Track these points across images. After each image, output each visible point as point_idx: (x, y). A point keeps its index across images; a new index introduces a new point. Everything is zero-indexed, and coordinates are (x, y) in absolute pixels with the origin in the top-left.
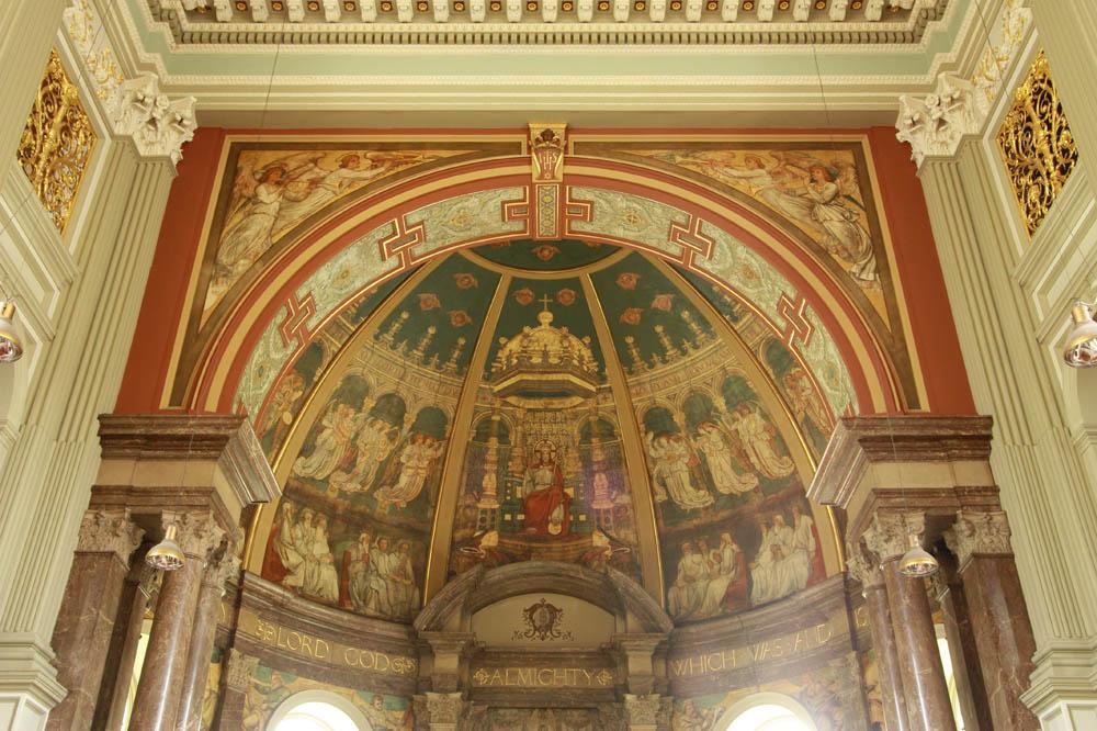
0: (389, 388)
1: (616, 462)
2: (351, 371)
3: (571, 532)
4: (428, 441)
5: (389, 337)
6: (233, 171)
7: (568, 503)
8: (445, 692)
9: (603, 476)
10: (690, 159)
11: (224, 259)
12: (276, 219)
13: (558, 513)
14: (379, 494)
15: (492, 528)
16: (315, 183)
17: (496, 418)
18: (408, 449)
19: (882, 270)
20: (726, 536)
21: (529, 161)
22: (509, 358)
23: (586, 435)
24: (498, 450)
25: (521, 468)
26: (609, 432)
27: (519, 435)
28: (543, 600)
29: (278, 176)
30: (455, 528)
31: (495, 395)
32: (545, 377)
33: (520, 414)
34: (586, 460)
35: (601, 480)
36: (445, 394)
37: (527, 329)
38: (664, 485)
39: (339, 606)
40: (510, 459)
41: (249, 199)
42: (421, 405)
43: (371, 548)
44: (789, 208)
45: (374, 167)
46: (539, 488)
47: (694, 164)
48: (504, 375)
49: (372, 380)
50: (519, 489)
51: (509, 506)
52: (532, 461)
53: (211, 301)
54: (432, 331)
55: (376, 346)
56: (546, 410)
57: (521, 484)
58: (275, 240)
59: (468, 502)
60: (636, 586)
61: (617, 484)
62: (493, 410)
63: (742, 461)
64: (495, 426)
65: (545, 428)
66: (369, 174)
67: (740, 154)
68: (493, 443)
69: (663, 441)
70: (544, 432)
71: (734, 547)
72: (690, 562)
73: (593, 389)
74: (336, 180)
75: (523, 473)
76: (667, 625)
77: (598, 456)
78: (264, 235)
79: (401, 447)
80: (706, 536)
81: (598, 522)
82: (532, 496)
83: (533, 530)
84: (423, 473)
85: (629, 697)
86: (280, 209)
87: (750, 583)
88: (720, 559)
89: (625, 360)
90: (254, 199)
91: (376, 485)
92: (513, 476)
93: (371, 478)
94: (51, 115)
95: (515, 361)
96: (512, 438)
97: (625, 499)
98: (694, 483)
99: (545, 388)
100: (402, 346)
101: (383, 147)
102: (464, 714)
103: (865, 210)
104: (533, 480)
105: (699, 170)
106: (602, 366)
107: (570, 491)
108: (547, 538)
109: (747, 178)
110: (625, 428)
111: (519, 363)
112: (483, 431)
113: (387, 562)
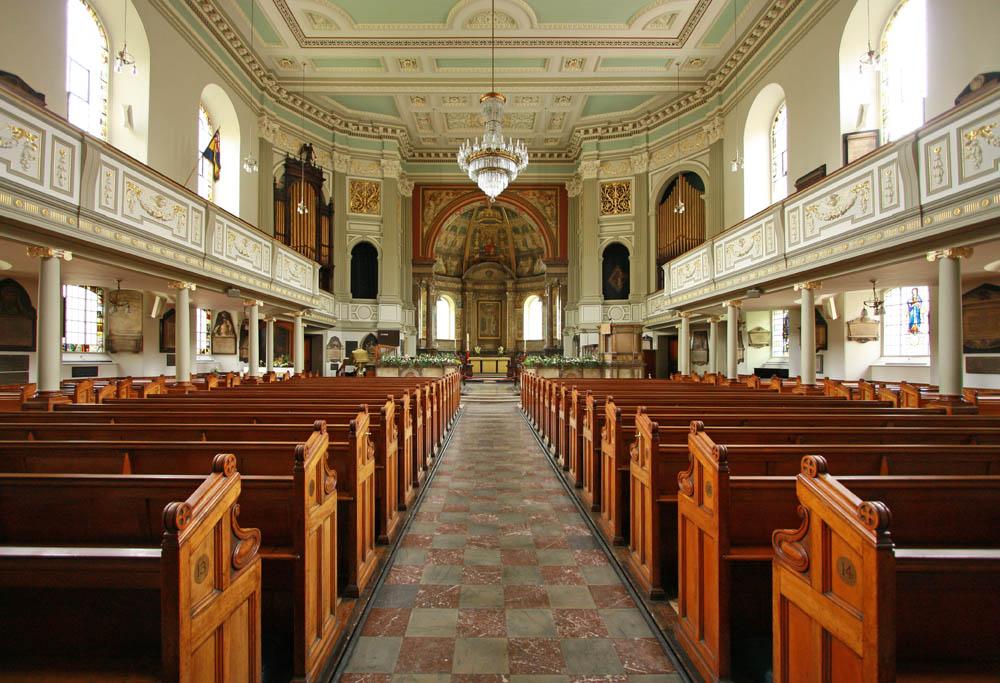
1: (505, 239)
6: (423, 197)
11: (426, 220)
13: (492, 250)
16: (441, 200)
19: (557, 224)
23: (499, 232)
26: (505, 232)
29: (433, 198)
34: (499, 238)
35: (502, 243)
39: (446, 275)
44: (539, 207)
51: (481, 248)
52: (486, 238)
53: (425, 231)
63: (534, 242)
67: (531, 192)
74: (446, 198)
77: (502, 237)
80: (525, 257)
81: (502, 252)
90: (429, 204)
101: (455, 190)
108: (489, 255)
110: (509, 231)
113: (455, 263)
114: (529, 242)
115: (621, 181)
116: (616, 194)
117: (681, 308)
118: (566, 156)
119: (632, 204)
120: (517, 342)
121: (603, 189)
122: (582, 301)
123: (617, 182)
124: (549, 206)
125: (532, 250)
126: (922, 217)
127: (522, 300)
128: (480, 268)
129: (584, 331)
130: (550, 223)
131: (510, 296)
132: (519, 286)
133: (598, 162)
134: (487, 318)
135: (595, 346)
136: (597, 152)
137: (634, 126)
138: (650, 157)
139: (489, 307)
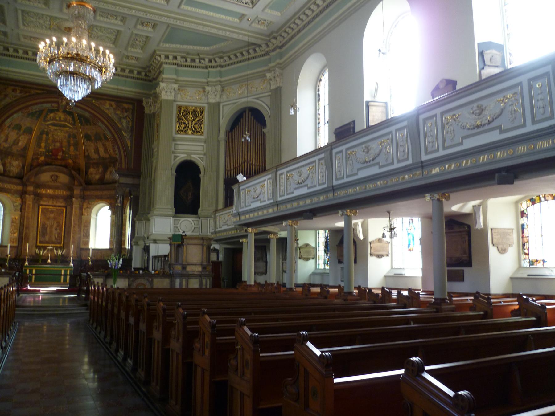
1: (76, 145)
3: (63, 159)
4: (27, 134)
7: (63, 152)
8: (29, 195)
9: (73, 147)
10: (96, 102)
13: (60, 154)
14: (14, 147)
15: (43, 156)
16: (6, 96)
17: (46, 130)
18: (22, 136)
19: (131, 136)
20: (101, 166)
21: (59, 98)
22: (50, 117)
24: (46, 138)
26: (75, 137)
28: (55, 174)
30: (34, 155)
33: (52, 130)
34: (69, 142)
35: (72, 148)
37: (56, 112)
38: (88, 151)
43: (11, 160)
45: (20, 93)
46: (56, 147)
47: (97, 103)
48: (48, 121)
52: (54, 141)
59: (37, 149)
60: (77, 175)
61: (76, 149)
63: (106, 150)
65: (58, 134)
66: (19, 95)
67: (108, 102)
68: (45, 136)
69: (89, 142)
71: (102, 169)
72: (92, 170)
73: (72, 127)
76: (84, 184)
77: (72, 142)
79: (20, 136)
80: (96, 165)
83: (53, 157)
84: (25, 142)
85: (74, 199)
87: (104, 177)
88: (99, 171)
89: (81, 122)
91: (14, 144)
93: (12, 143)
96: (50, 135)
97: (77, 153)
98: (95, 153)
101: (24, 87)
102: (34, 199)
103: (132, 121)
104: (54, 146)
105: (98, 105)
106: (75, 122)
107: (64, 149)
108: (57, 159)
109: (108, 109)
112: (42, 133)
114: (101, 150)
115: (196, 107)
116: (190, 117)
117: (248, 225)
118: (146, 75)
119: (205, 128)
120: (81, 249)
121: (180, 111)
122: (155, 212)
123: (192, 106)
124: (125, 118)
125: (103, 158)
126: (422, 169)
127: (90, 208)
128: (44, 171)
129: (155, 241)
130: (125, 134)
131: (76, 203)
132: (87, 193)
133: (176, 86)
134: (49, 223)
135: (165, 256)
136: (175, 77)
137: (210, 61)
138: (223, 90)
139: (52, 212)
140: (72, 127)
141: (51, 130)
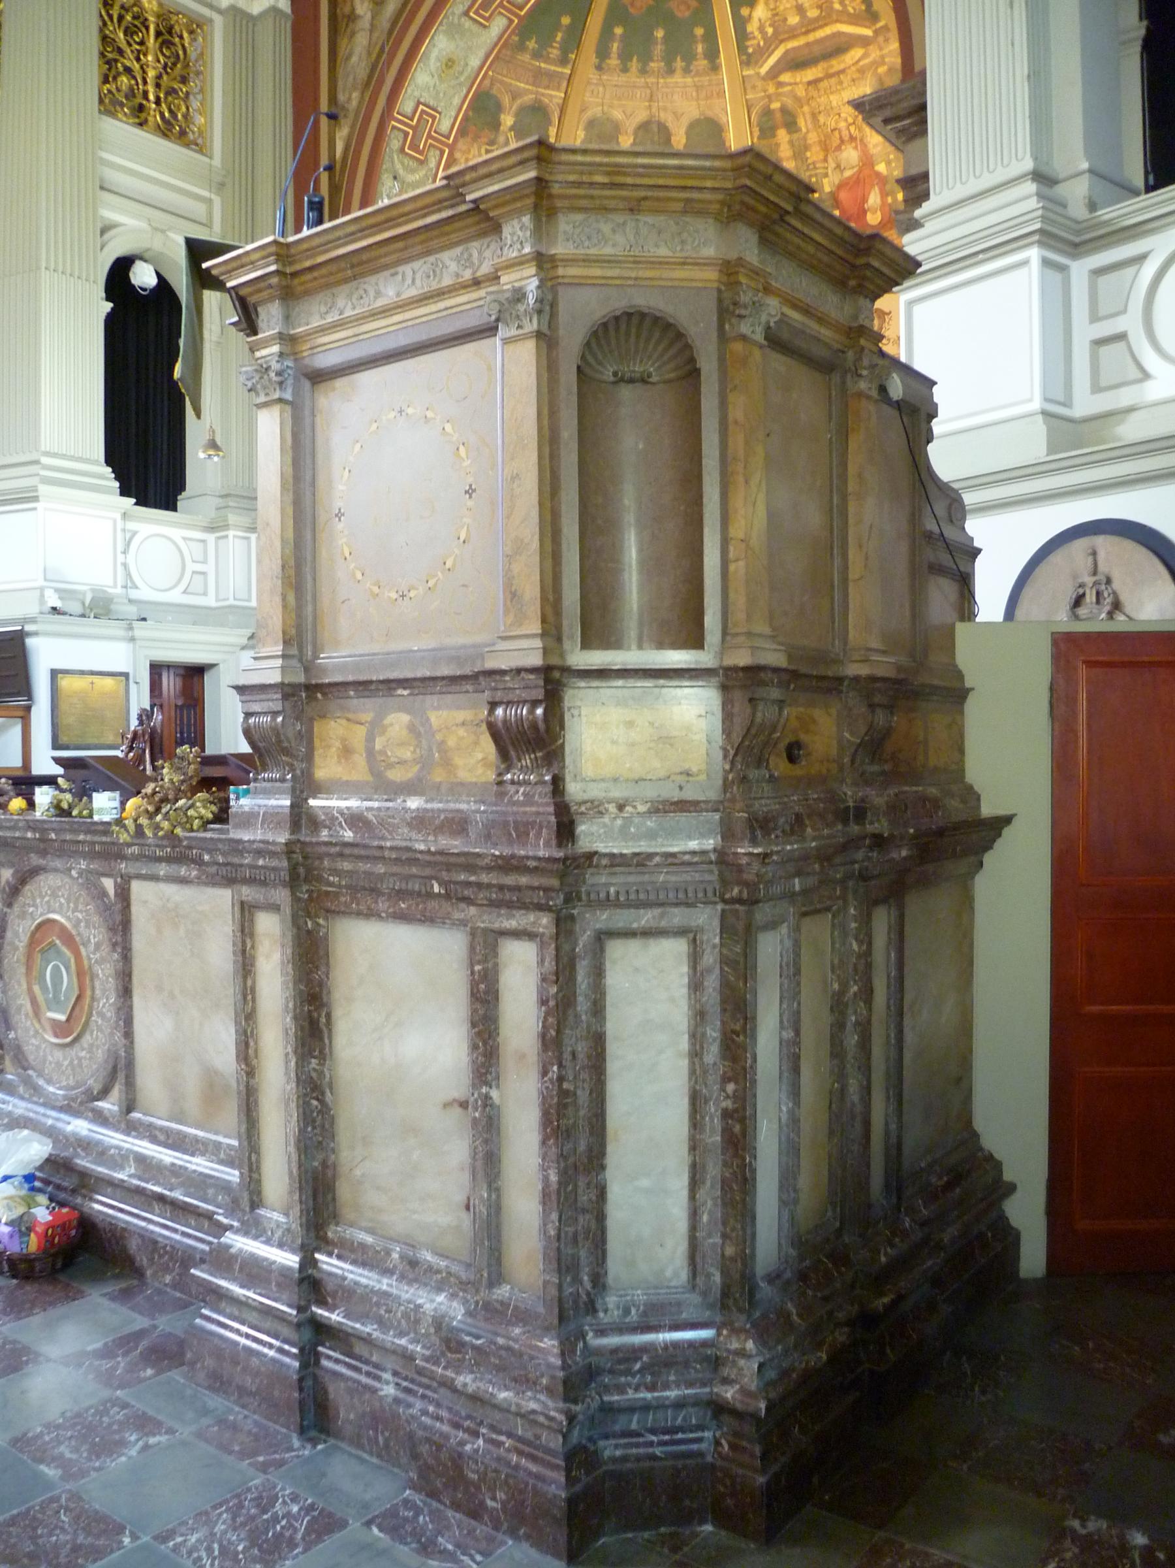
0: (642, 116)
2: (589, 114)
5: (614, 61)
11: (342, 98)
12: (371, 31)
17: (775, 105)
22: (761, 29)
24: (791, 142)
25: (821, 156)
27: (808, 117)
31: (764, 79)
32: (811, 37)
33: (801, 92)
36: (707, 98)
40: (807, 148)
41: (349, 17)
42: (685, 122)
46: (848, 174)
48: (763, 52)
49: (617, 115)
50: (825, 181)
54: (660, 34)
55: (605, 77)
56: (829, 76)
57: (826, 175)
58: (374, 56)
62: (769, 97)
64: (778, 115)
68: (782, 135)
70: (834, 104)
73: (868, 32)
75: (825, 160)
78: (364, 56)
82: (840, 187)
86: (373, 18)
90: (352, 17)
92: (815, 168)
94: (142, 43)
95: (770, 31)
96: (801, 123)
99: (817, 50)
100: (634, 64)
104: (838, 166)
111: (776, 33)
140: (868, 32)
141: (797, 99)
